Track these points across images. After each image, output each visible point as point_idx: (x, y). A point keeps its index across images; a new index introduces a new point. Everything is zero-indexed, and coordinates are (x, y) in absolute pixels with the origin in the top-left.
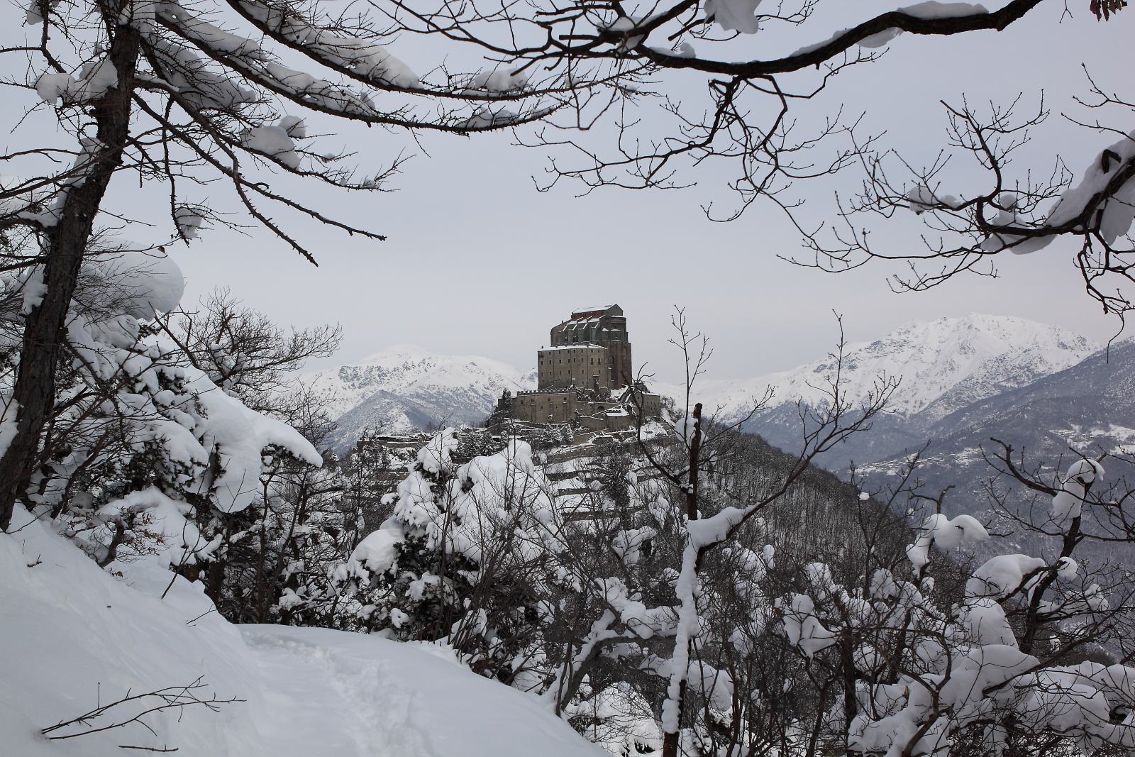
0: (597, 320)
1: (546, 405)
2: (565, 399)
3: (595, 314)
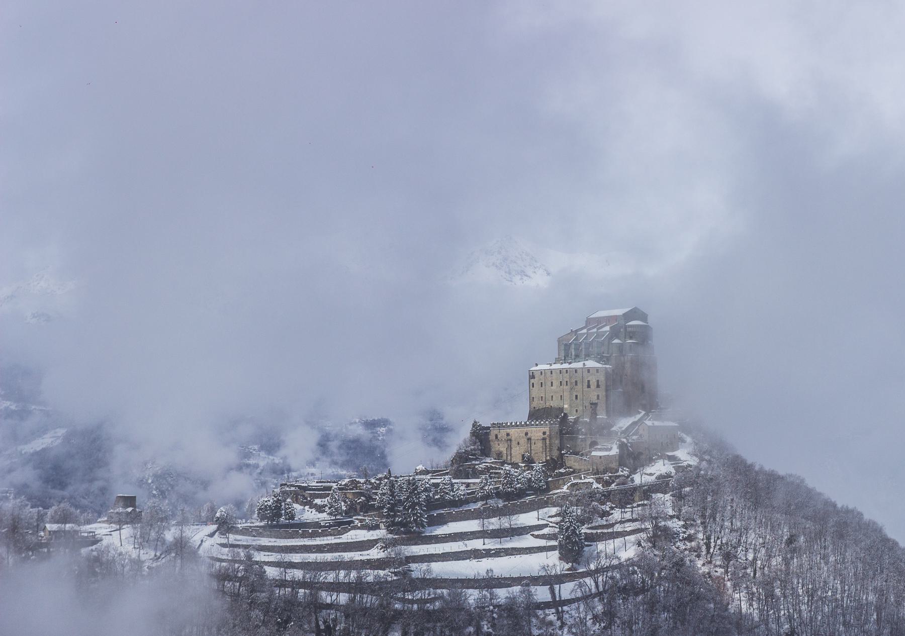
0: (607, 328)
1: (523, 441)
2: (544, 433)
3: (609, 319)
